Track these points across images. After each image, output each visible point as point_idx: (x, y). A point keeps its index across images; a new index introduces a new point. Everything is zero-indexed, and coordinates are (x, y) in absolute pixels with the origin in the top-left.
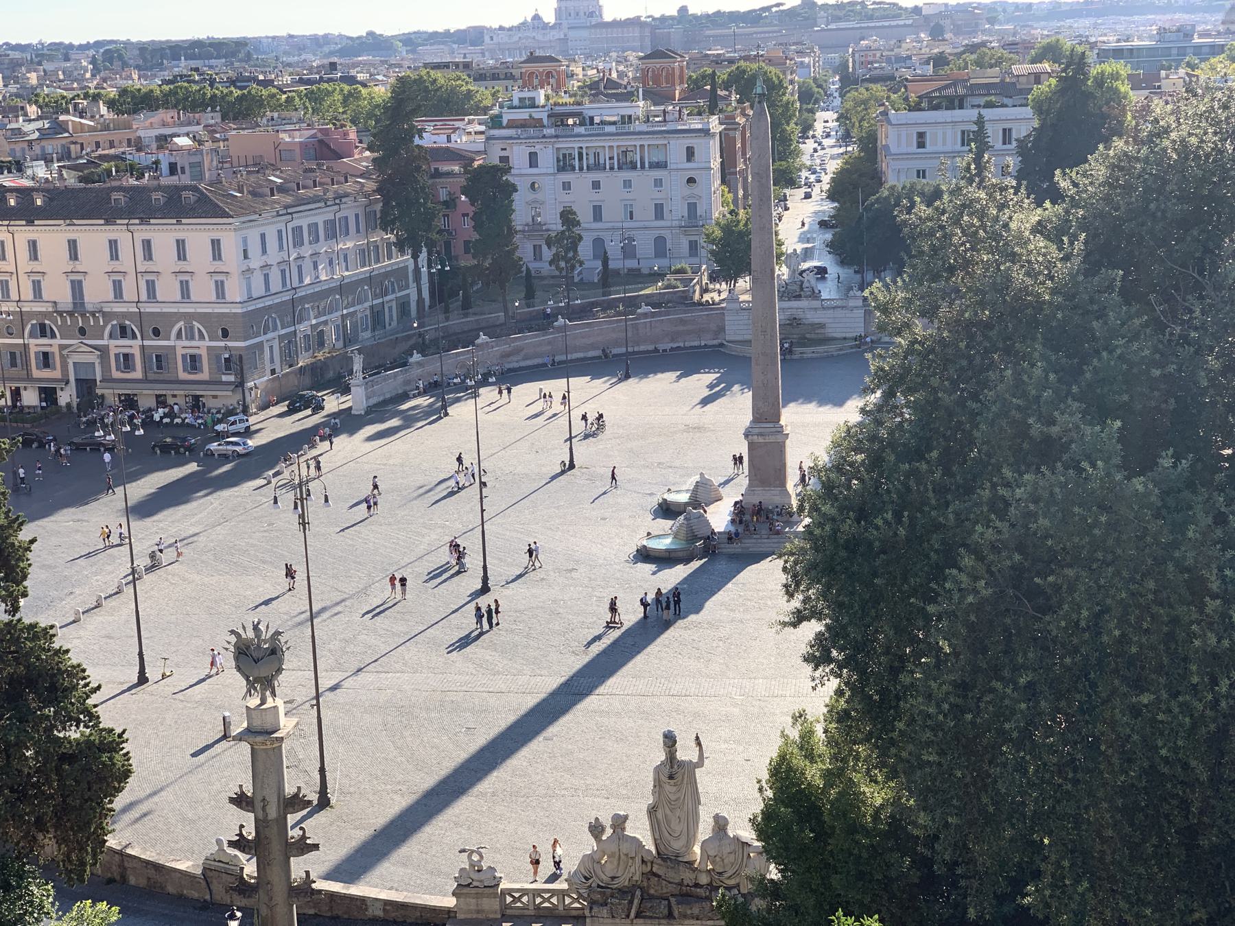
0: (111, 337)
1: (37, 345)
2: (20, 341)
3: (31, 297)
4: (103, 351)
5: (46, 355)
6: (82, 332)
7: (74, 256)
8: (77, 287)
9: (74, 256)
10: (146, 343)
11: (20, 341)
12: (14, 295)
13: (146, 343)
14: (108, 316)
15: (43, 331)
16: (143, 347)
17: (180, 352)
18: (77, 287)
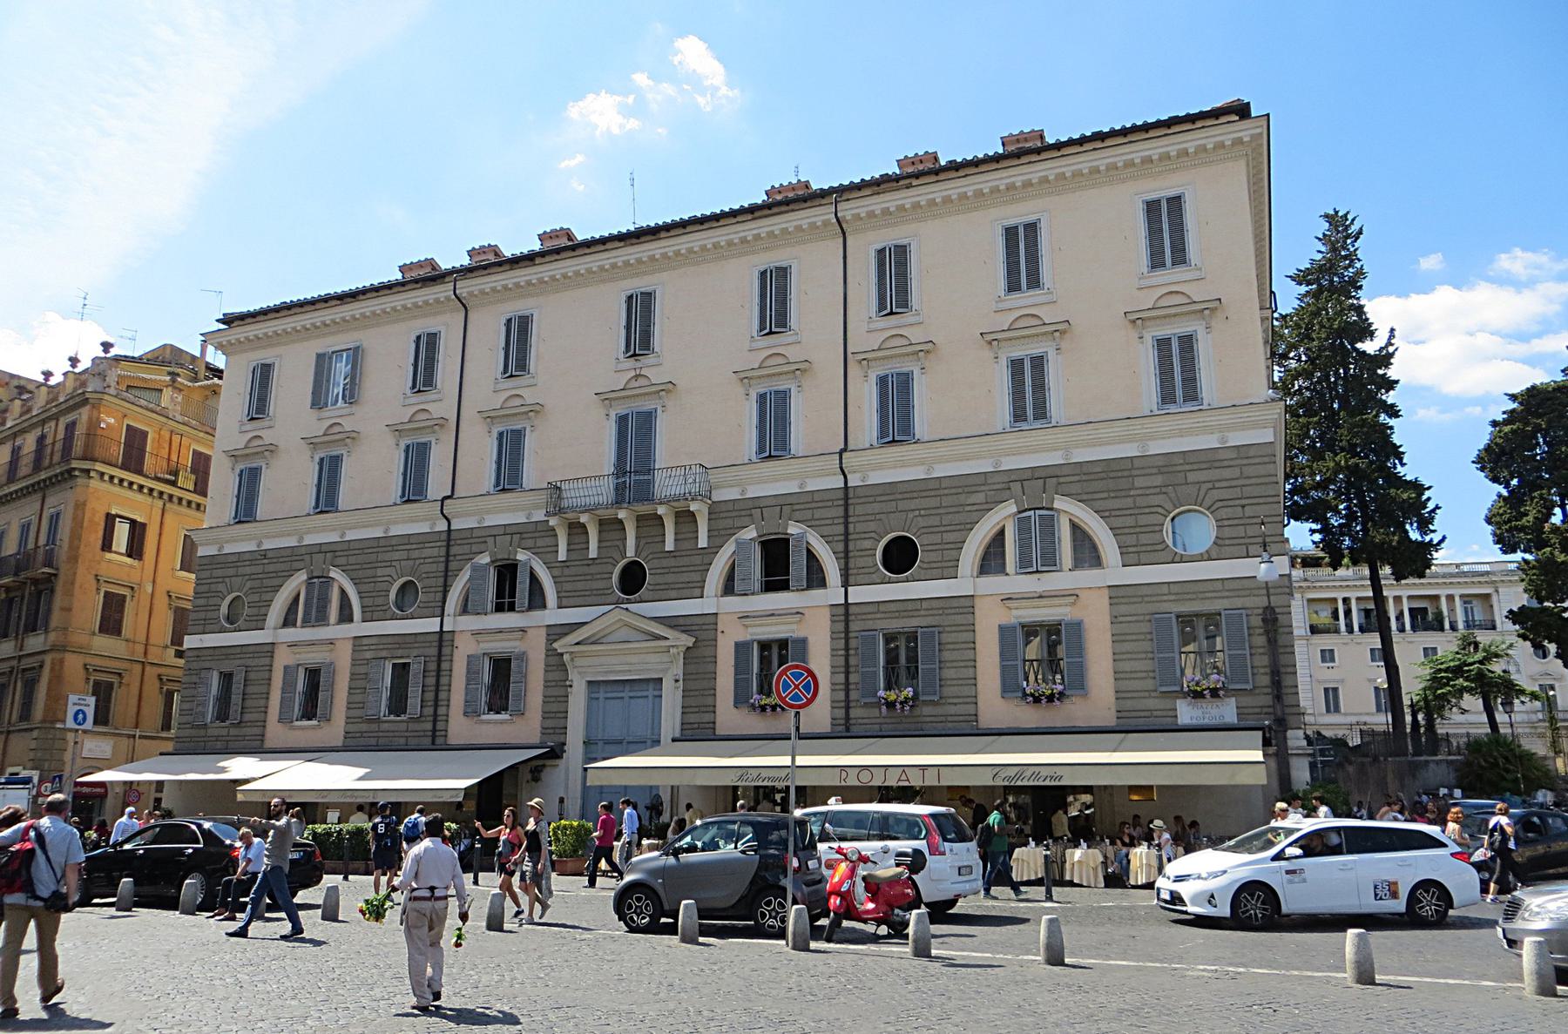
0: (729, 589)
1: (476, 632)
2: (432, 625)
3: (488, 482)
4: (702, 630)
5: (502, 667)
6: (632, 580)
7: (639, 339)
8: (635, 435)
9: (639, 339)
10: (858, 594)
11: (432, 625)
12: (437, 484)
13: (858, 594)
14: (726, 517)
15: (509, 588)
16: (845, 613)
17: (988, 624)
18: (635, 435)
